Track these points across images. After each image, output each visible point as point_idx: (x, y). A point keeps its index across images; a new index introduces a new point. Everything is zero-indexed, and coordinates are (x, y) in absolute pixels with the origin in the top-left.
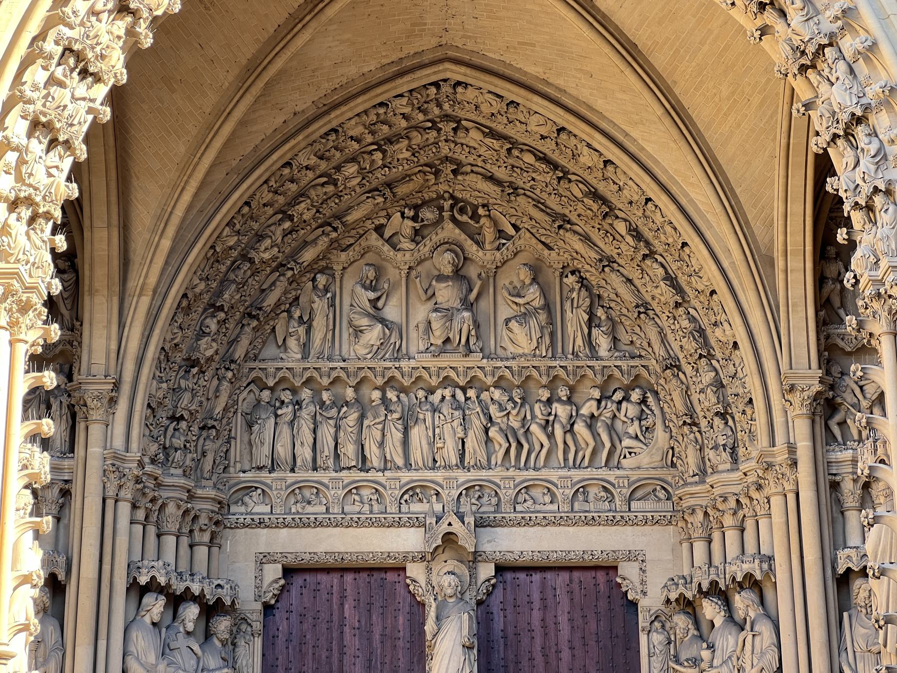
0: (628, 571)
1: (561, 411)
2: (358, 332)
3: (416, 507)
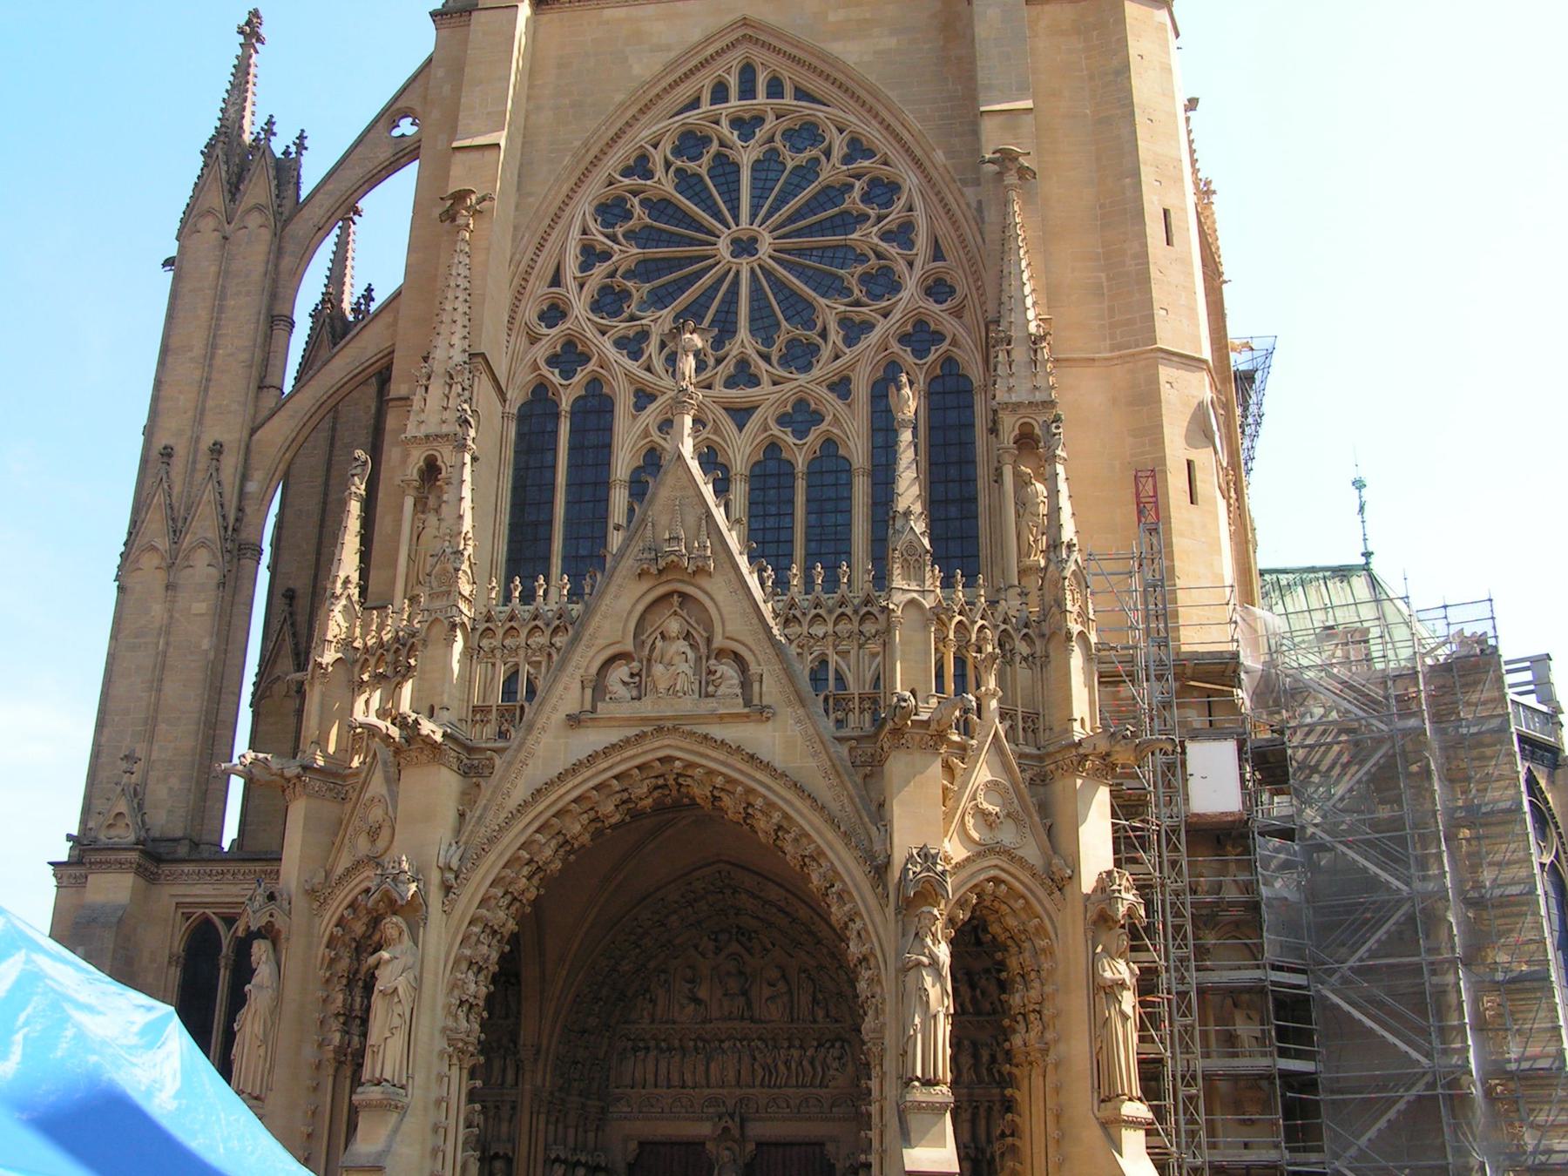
0: (830, 1148)
1: (795, 1053)
2: (682, 1007)
3: (711, 1110)
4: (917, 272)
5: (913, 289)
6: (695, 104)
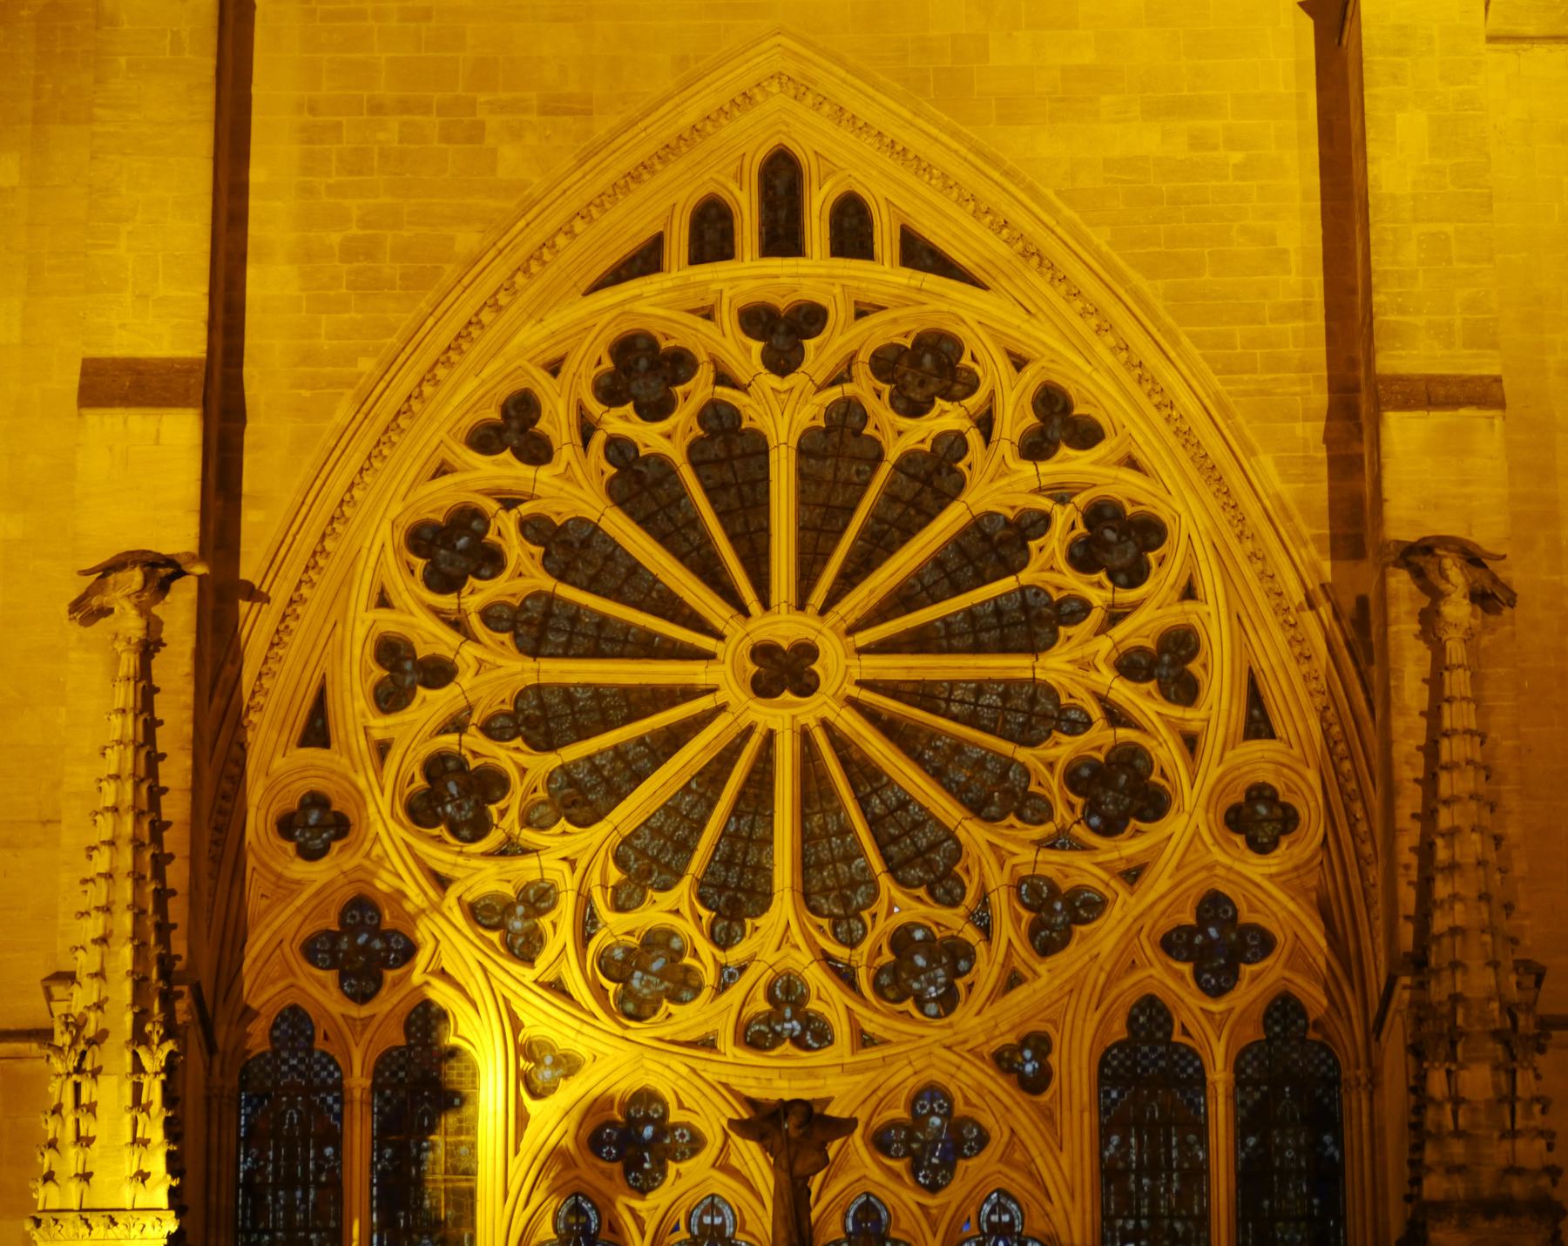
4: (1211, 772)
5: (1199, 817)
6: (647, 260)
